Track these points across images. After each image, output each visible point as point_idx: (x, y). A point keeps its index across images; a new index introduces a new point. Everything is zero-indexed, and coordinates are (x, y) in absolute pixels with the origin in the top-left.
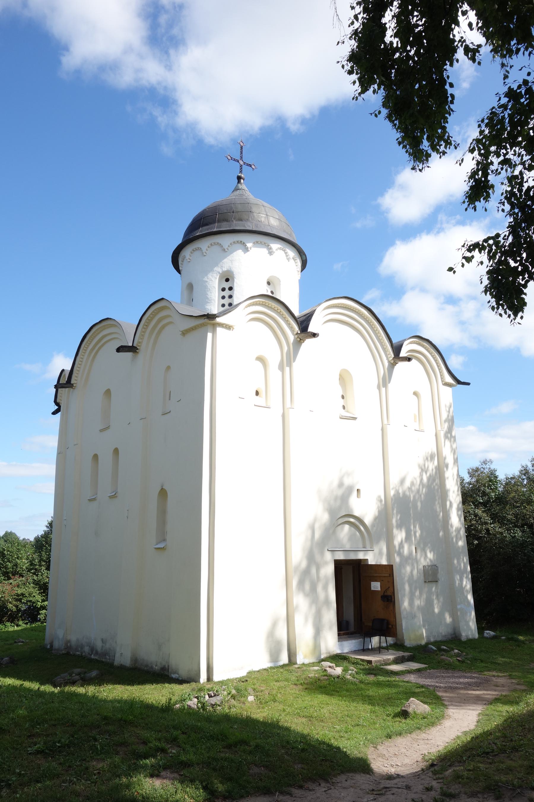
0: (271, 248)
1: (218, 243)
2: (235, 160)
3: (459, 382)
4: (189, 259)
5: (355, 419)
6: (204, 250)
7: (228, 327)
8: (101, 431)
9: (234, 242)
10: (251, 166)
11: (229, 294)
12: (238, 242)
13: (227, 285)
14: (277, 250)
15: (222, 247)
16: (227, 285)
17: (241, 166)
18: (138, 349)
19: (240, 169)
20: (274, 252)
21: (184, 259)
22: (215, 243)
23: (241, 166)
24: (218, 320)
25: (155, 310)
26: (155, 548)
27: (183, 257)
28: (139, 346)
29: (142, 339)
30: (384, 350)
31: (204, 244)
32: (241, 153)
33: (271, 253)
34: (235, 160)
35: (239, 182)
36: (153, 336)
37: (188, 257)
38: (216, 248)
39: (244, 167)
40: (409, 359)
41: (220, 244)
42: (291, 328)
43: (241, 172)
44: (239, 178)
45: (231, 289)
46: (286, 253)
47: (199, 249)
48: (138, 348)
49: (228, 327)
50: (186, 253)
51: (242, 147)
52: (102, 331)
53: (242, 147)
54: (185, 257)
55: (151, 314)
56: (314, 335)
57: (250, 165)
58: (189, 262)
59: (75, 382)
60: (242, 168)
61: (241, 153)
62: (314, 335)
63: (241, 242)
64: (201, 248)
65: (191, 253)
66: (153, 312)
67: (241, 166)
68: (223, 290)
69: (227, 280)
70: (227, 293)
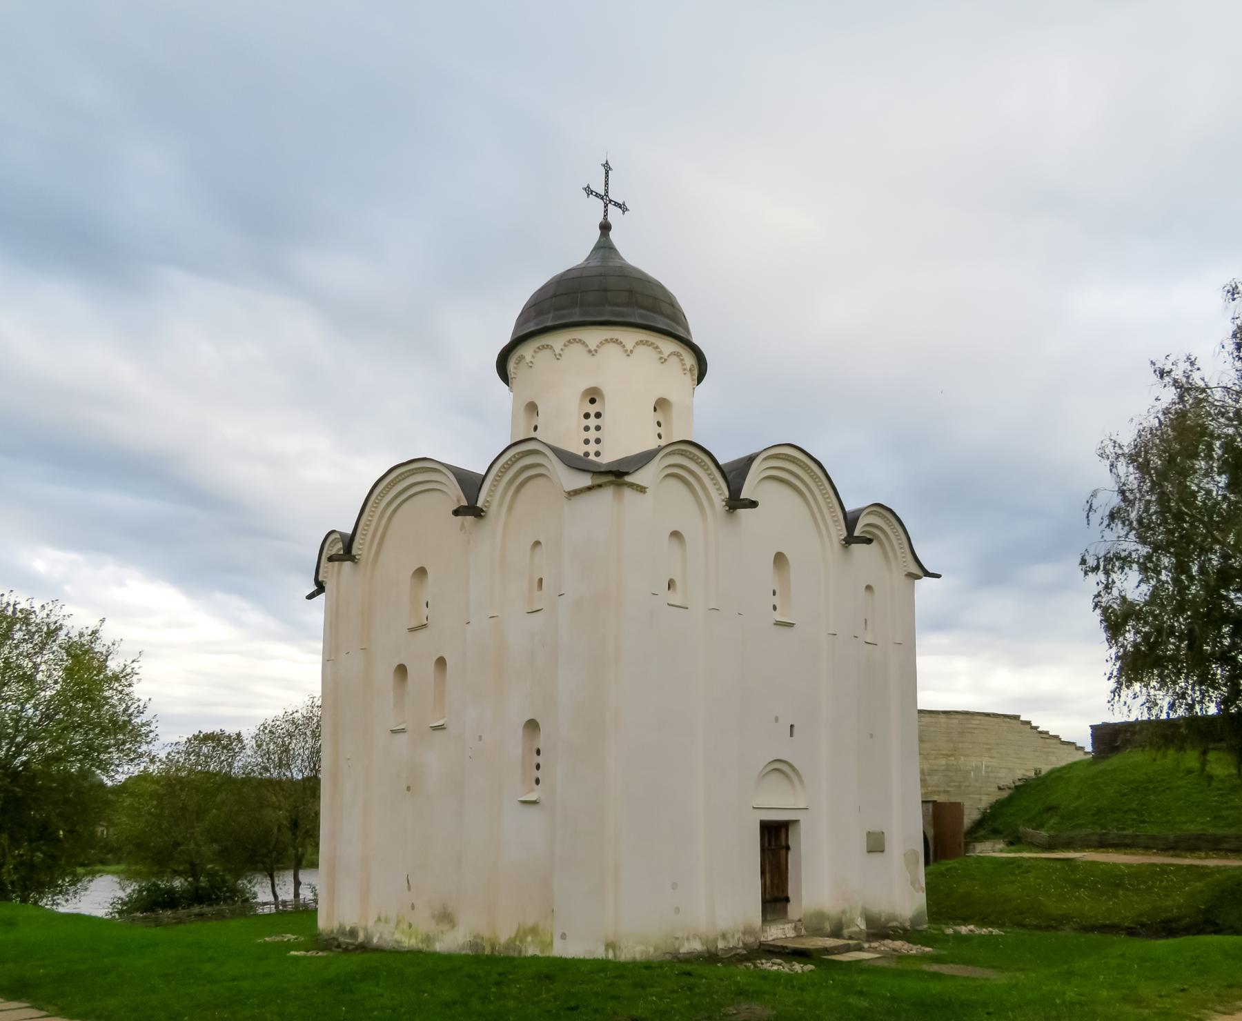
0: (660, 352)
1: (580, 340)
2: (597, 195)
4: (531, 362)
6: (558, 351)
8: (412, 630)
9: (606, 340)
10: (620, 207)
11: (596, 424)
12: (612, 339)
13: (592, 409)
14: (669, 356)
15: (587, 346)
16: (592, 409)
17: (606, 206)
18: (483, 511)
19: (605, 212)
20: (665, 360)
21: (520, 361)
22: (575, 340)
24: (628, 479)
25: (518, 454)
27: (519, 357)
28: (486, 507)
29: (491, 496)
31: (557, 340)
32: (607, 183)
34: (597, 195)
36: (510, 493)
37: (528, 358)
38: (576, 349)
41: (584, 342)
43: (606, 215)
44: (605, 227)
45: (598, 415)
46: (682, 360)
47: (548, 347)
48: (484, 509)
50: (527, 351)
52: (408, 476)
54: (522, 358)
55: (510, 459)
57: (619, 204)
58: (531, 367)
59: (360, 552)
60: (607, 210)
61: (607, 183)
63: (617, 340)
64: (552, 347)
65: (535, 352)
66: (514, 456)
67: (605, 207)
68: (587, 416)
69: (593, 401)
70: (592, 422)
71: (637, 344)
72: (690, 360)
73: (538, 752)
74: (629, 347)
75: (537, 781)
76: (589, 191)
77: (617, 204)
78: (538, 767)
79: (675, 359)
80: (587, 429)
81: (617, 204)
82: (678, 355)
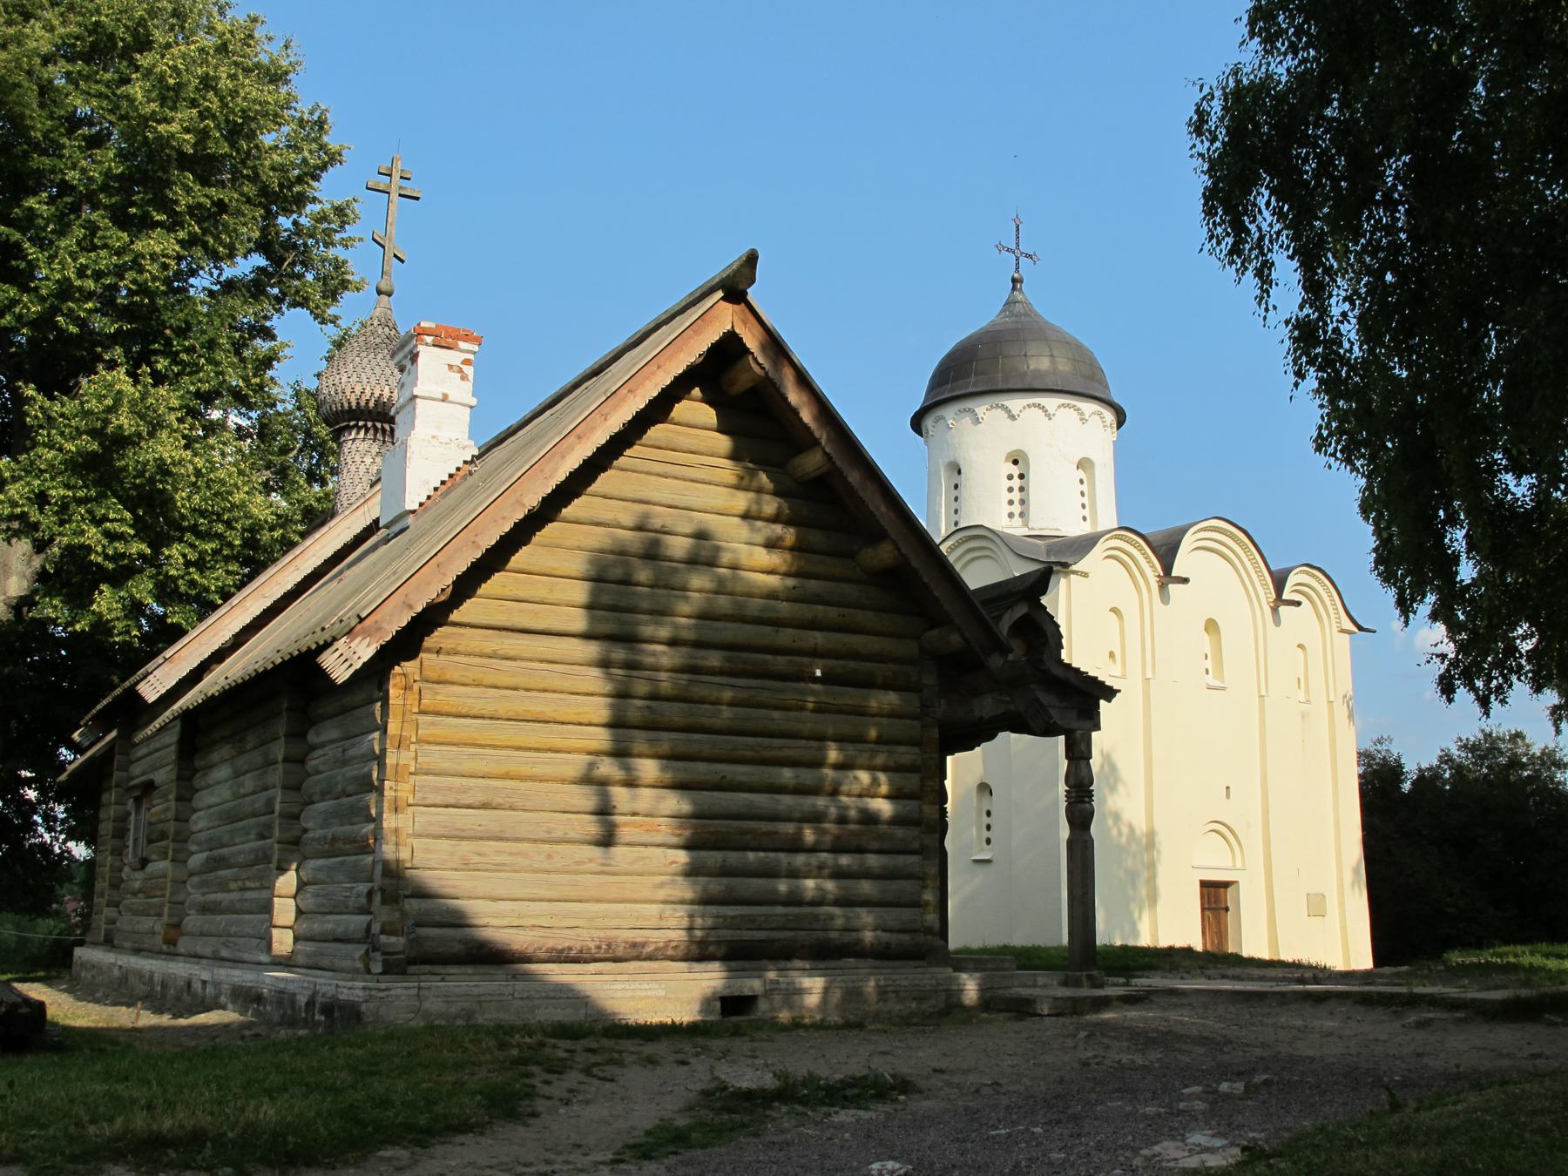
0: (1083, 414)
3: (1361, 628)
5: (1224, 689)
7: (1085, 575)
17: (1017, 259)
23: (1017, 259)
24: (1074, 568)
26: (976, 861)
30: (1264, 585)
33: (1083, 420)
35: (1014, 289)
39: (1022, 260)
40: (1298, 604)
42: (1153, 566)
44: (1014, 281)
49: (1085, 575)
51: (1018, 227)
53: (1018, 227)
56: (1185, 581)
62: (1185, 581)
68: (1010, 477)
71: (1059, 407)
72: (1109, 417)
73: (989, 814)
74: (1051, 411)
75: (988, 841)
76: (1000, 248)
77: (1029, 256)
78: (989, 827)
79: (1097, 418)
80: (1010, 490)
81: (1029, 256)
82: (1100, 414)
